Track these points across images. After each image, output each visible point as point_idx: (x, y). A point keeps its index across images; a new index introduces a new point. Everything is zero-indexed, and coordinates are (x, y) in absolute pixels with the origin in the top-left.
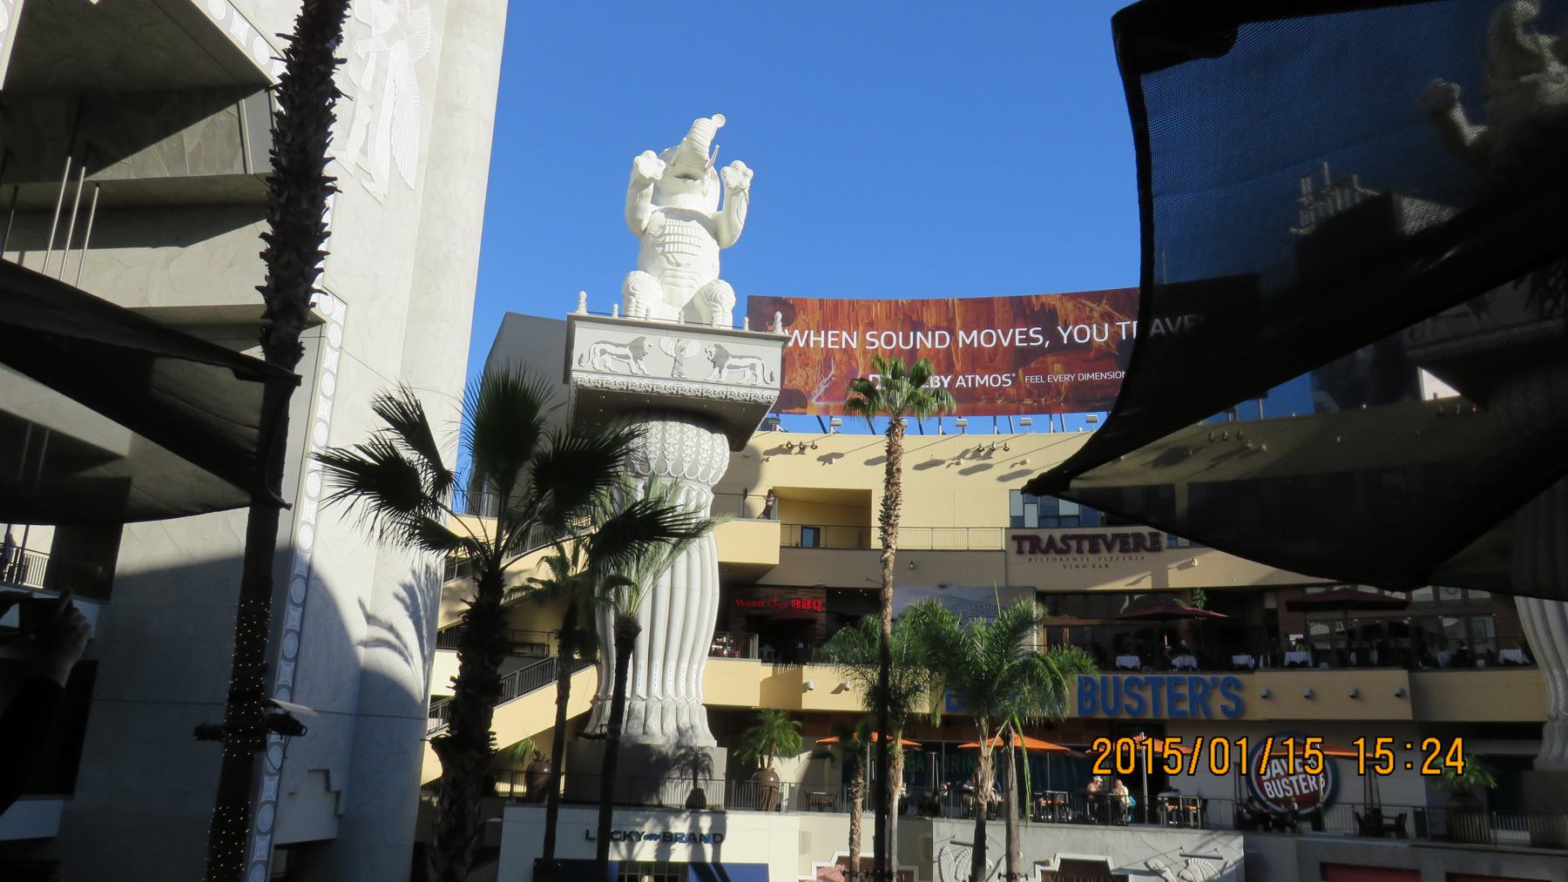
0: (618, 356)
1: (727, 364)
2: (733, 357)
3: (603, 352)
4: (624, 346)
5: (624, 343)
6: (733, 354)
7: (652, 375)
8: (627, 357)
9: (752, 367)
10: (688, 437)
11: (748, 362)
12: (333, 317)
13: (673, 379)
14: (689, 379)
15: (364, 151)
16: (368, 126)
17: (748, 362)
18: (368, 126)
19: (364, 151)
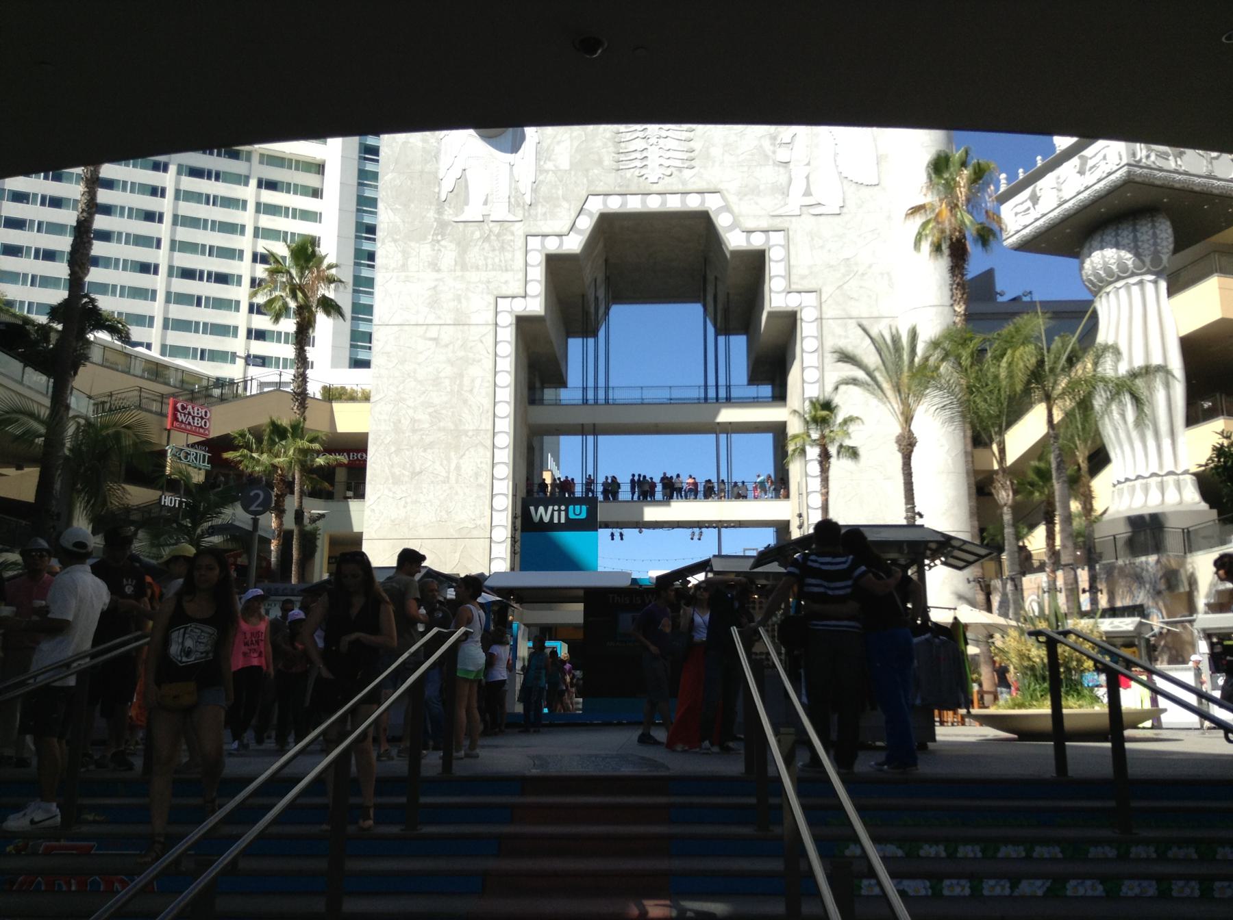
0: (1025, 211)
1: (1088, 168)
2: (1091, 158)
3: (1016, 214)
4: (1026, 201)
5: (1024, 199)
6: (1090, 156)
7: (1046, 212)
8: (1029, 209)
9: (1105, 158)
10: (1142, 233)
11: (1100, 156)
12: (802, 305)
13: (1060, 205)
14: (1068, 198)
15: (808, 193)
16: (807, 177)
17: (1100, 156)
18: (807, 177)
19: (808, 193)
